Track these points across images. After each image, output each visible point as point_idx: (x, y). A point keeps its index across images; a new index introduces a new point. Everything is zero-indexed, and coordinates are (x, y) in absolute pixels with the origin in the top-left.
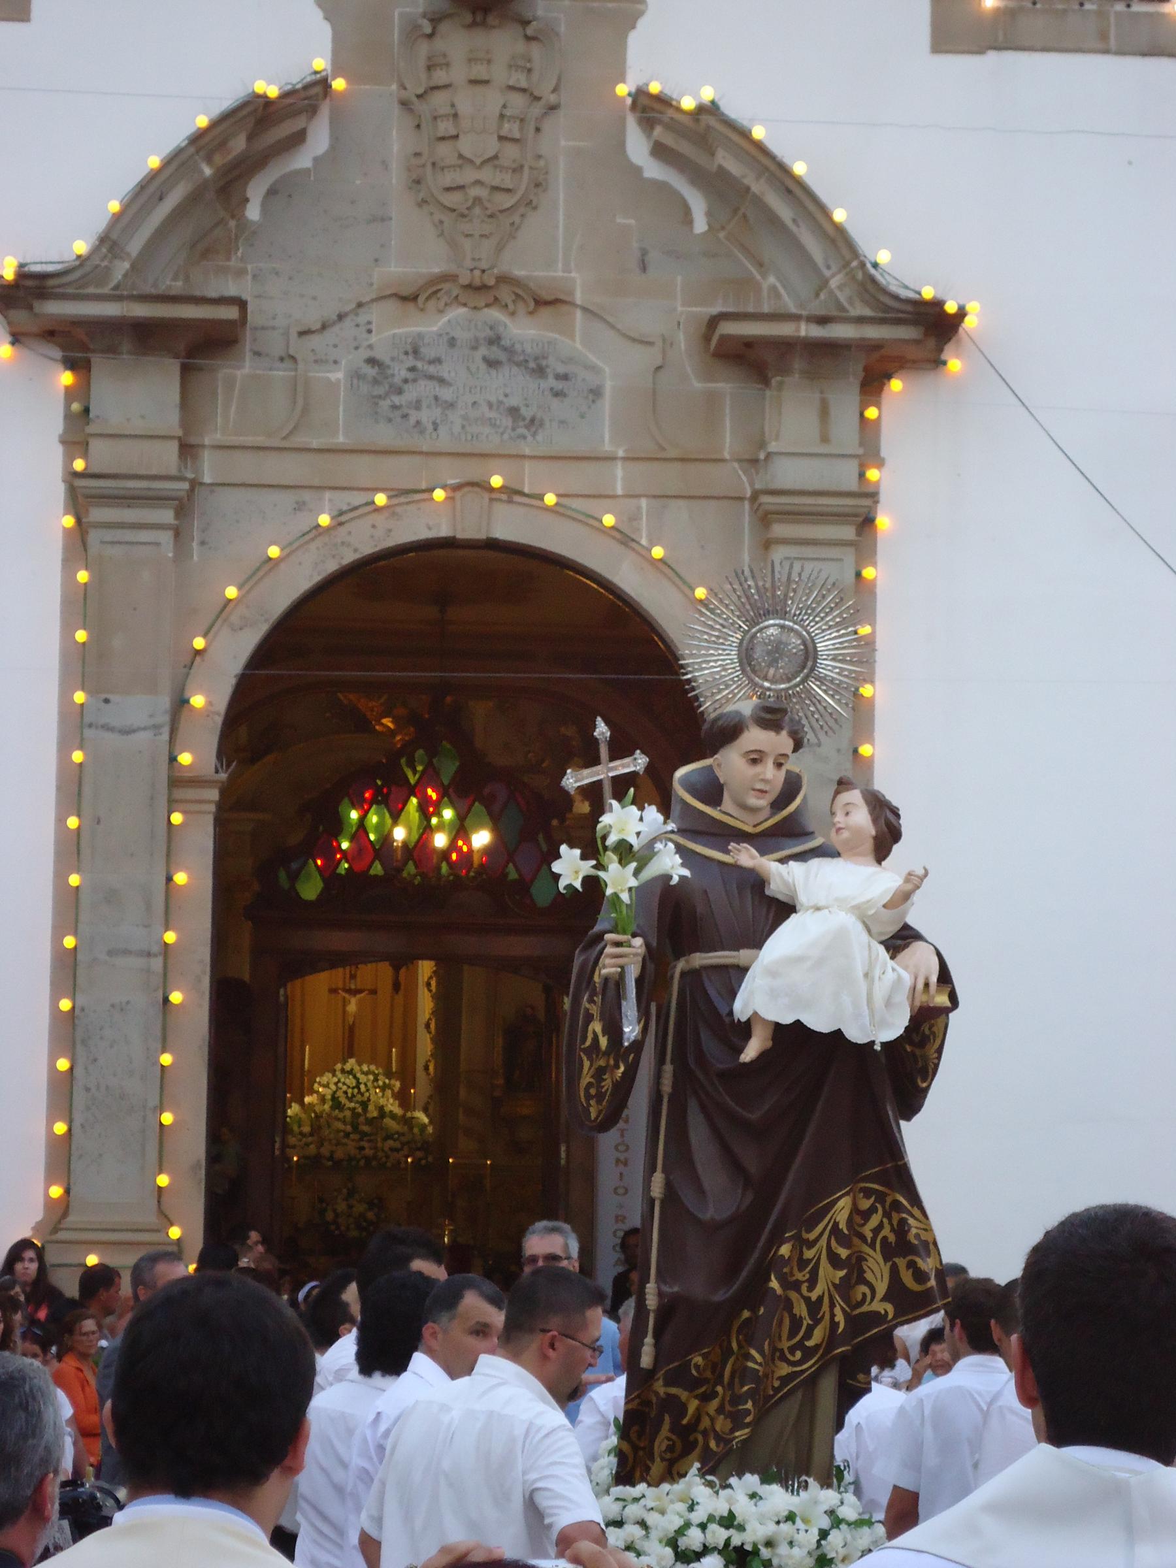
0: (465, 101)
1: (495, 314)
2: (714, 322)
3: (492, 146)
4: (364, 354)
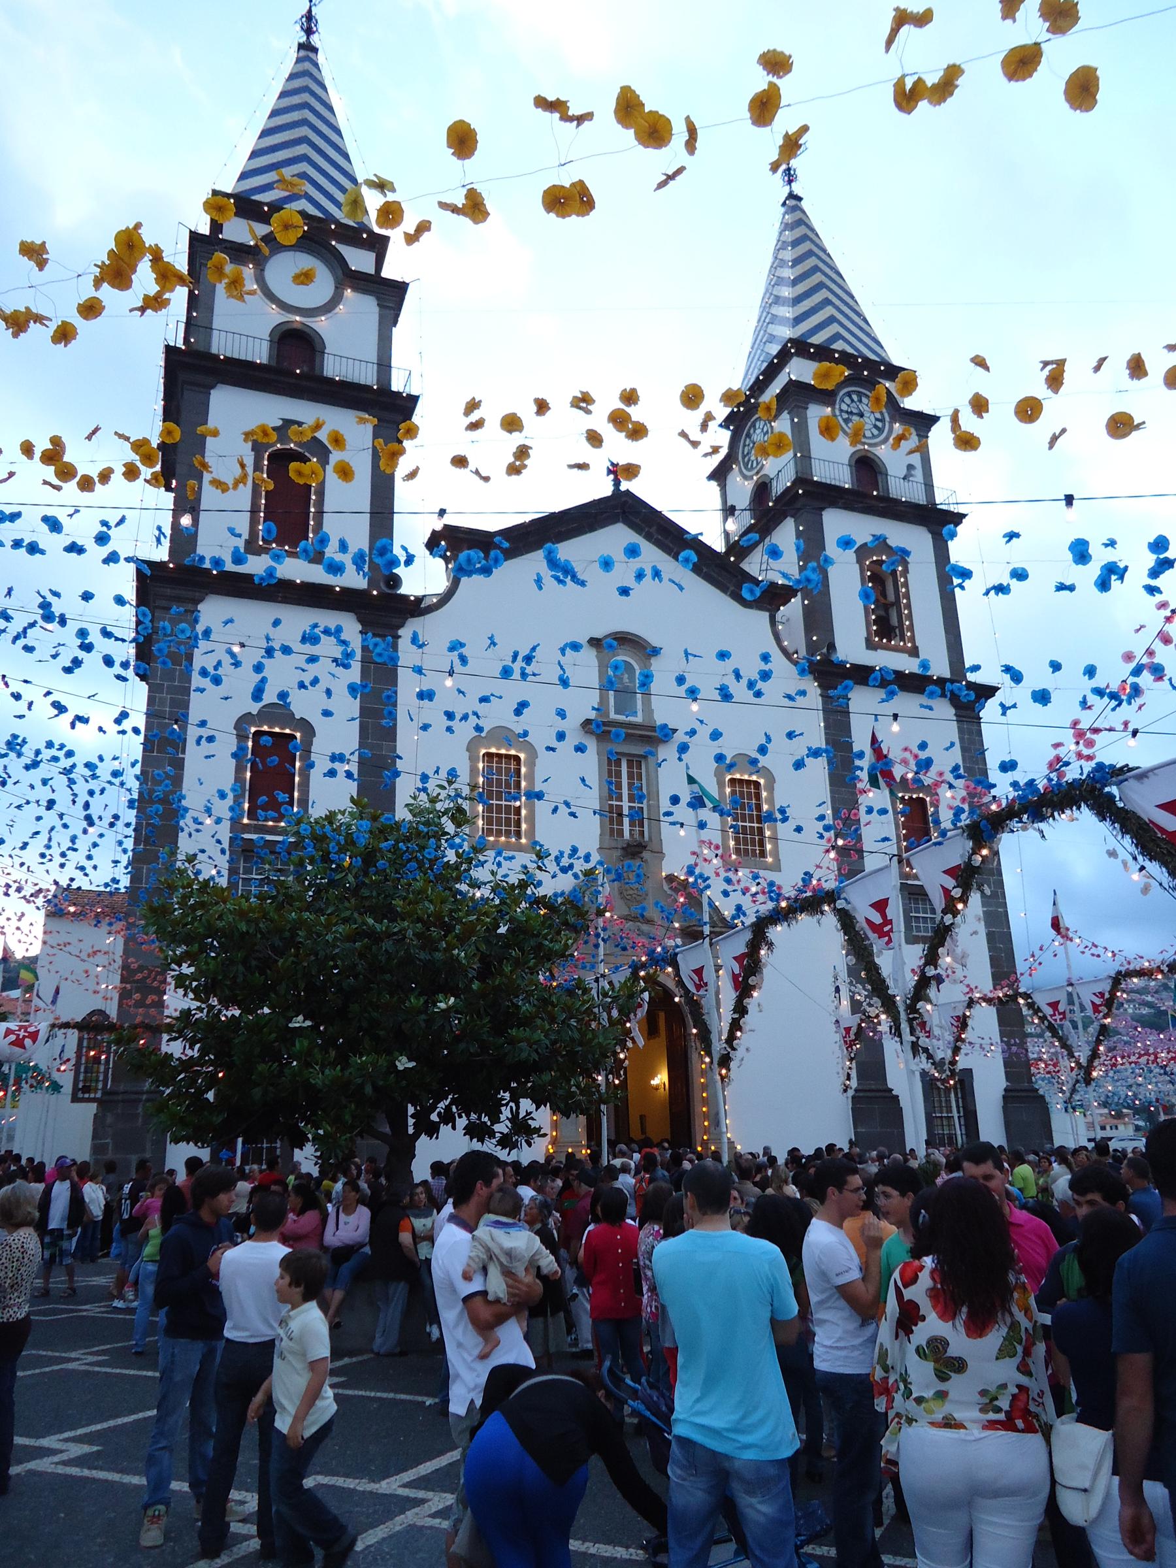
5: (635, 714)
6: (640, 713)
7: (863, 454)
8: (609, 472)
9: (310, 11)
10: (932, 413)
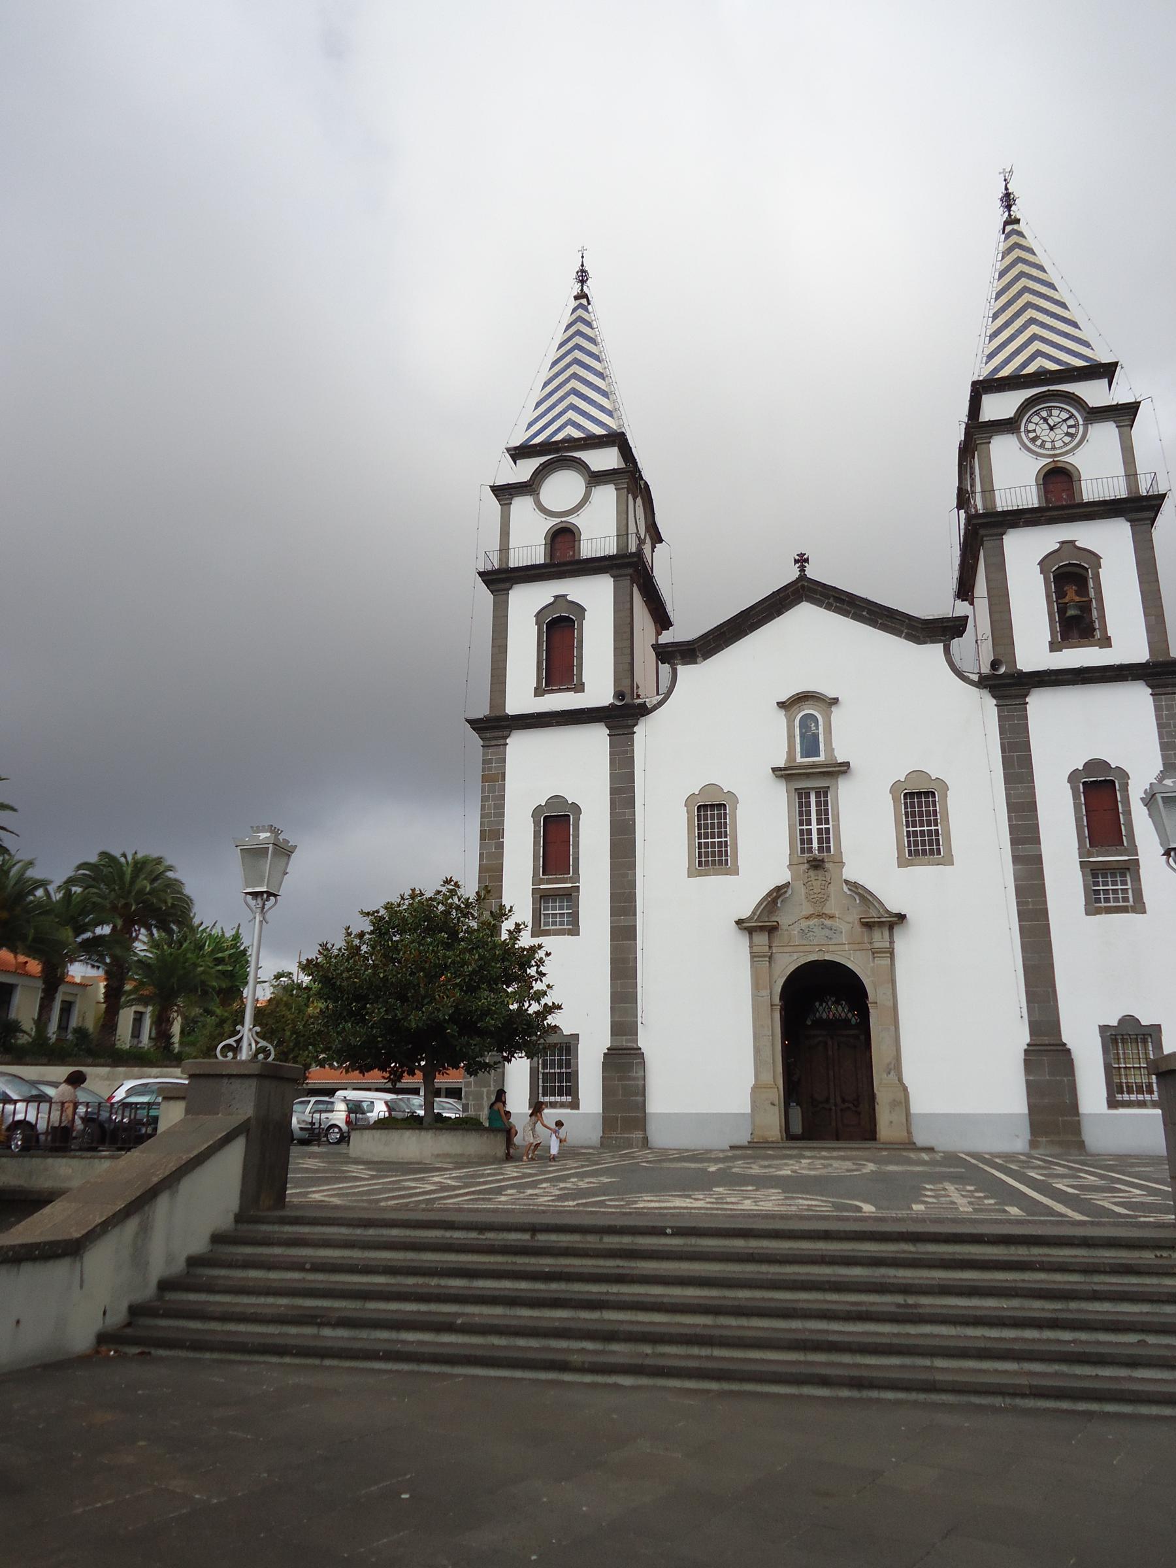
0: (814, 883)
1: (823, 920)
2: (860, 919)
3: (820, 891)
4: (799, 929)
5: (819, 756)
6: (822, 753)
7: (1052, 466)
8: (796, 561)
9: (582, 265)
10: (1133, 400)
